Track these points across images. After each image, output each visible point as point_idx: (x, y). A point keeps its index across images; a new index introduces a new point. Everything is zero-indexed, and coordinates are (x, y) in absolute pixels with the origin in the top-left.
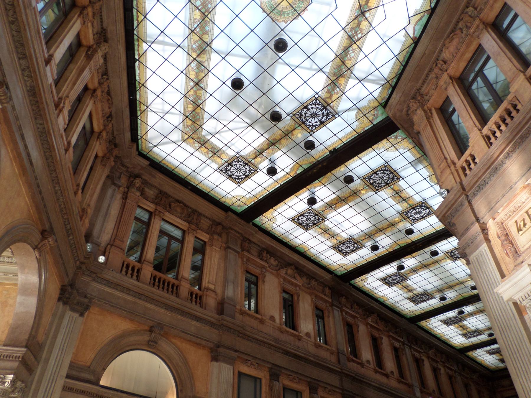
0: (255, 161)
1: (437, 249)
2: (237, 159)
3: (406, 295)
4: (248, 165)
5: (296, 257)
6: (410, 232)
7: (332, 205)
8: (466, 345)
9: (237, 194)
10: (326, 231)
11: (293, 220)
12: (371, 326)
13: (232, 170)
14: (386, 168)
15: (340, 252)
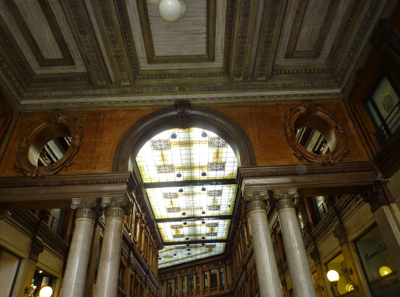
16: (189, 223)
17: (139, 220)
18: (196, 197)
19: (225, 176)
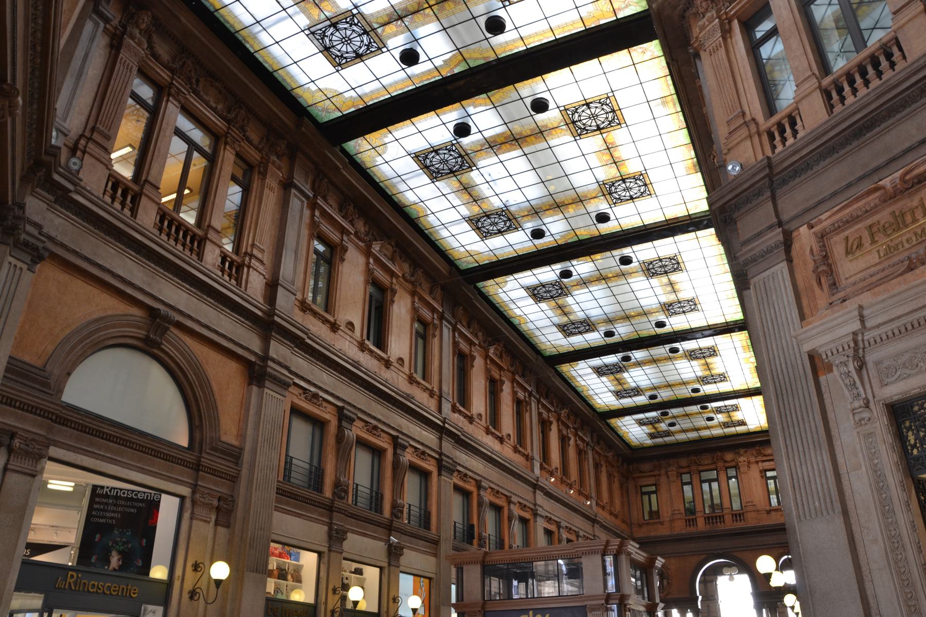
0: (383, 31)
1: (632, 255)
2: (352, 17)
3: (556, 320)
4: (368, 35)
5: (401, 226)
7: (494, 145)
8: (612, 408)
9: (328, 87)
10: (467, 189)
11: (417, 157)
12: (492, 361)
13: (334, 38)
14: (608, 101)
15: (478, 229)
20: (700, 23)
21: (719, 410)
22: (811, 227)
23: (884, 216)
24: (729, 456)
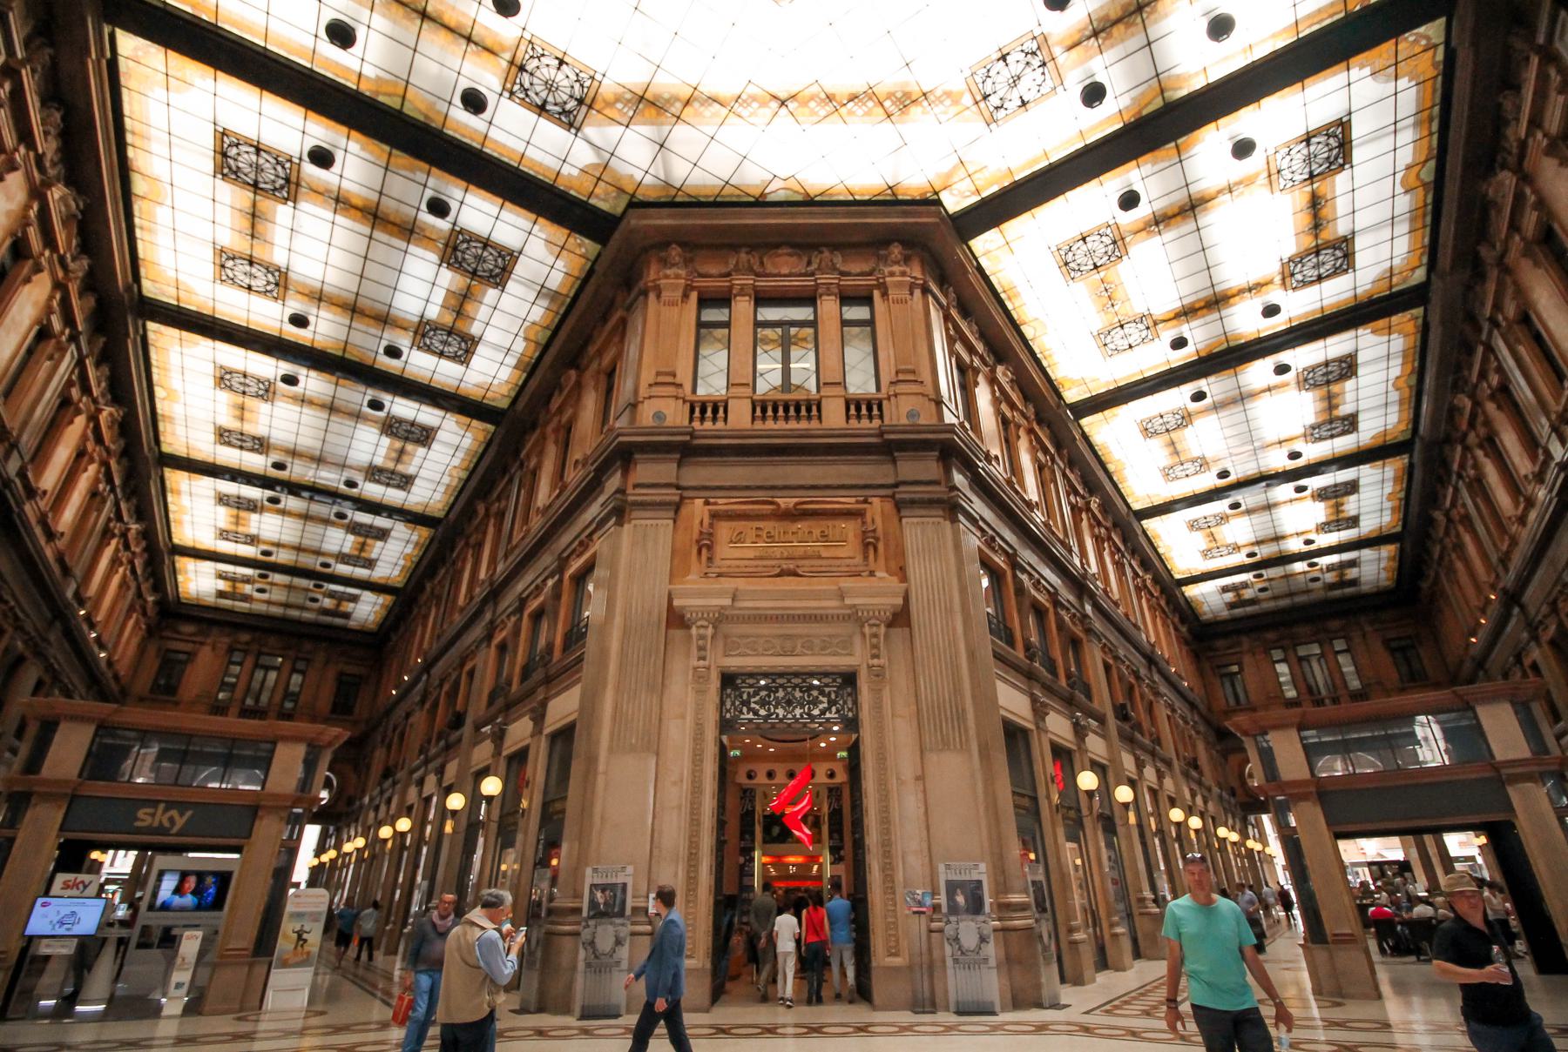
1: (387, 404)
6: (393, 352)
7: (341, 202)
16: (1248, 497)
17: (1084, 516)
18: (1260, 409)
19: (1359, 291)
20: (668, 272)
21: (332, 595)
22: (707, 503)
23: (767, 526)
24: (308, 646)
